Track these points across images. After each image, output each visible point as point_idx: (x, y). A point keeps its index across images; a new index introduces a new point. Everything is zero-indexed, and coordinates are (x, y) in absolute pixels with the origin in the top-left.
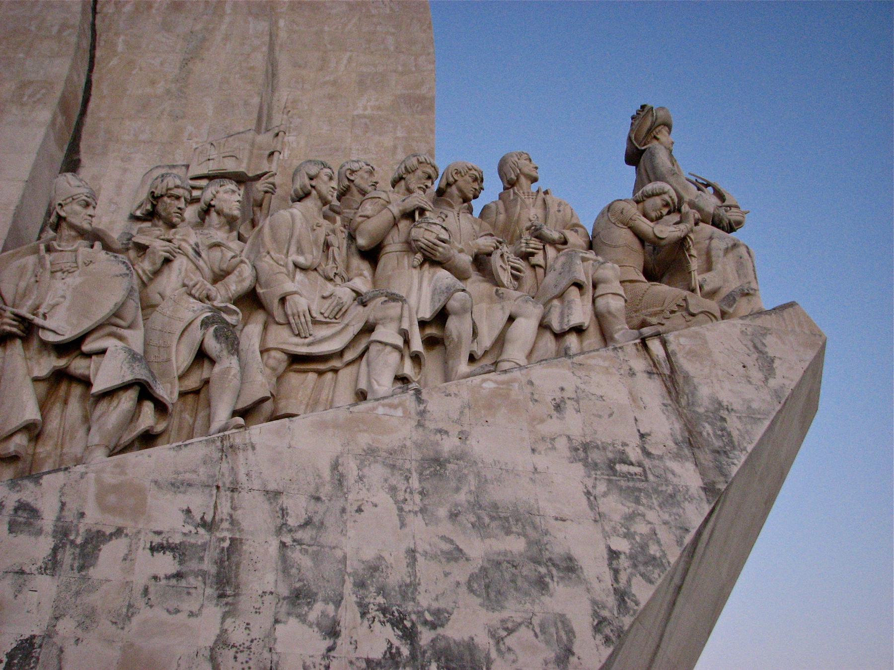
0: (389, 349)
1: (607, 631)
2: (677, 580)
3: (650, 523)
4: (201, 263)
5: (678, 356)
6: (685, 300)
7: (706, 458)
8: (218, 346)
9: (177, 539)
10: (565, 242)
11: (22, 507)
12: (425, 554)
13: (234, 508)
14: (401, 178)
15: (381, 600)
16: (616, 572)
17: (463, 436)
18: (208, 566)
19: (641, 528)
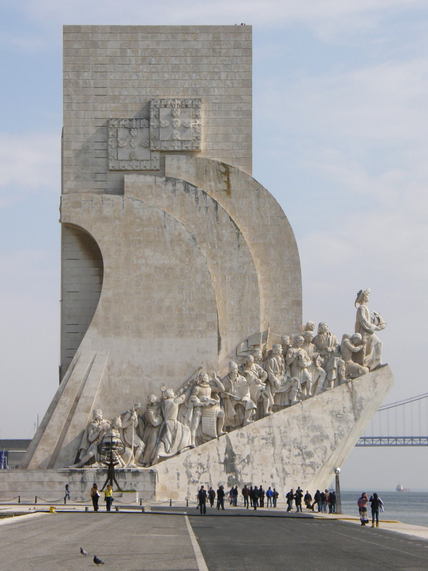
1: (333, 448)
2: (347, 436)
3: (342, 427)
4: (257, 374)
5: (355, 386)
6: (359, 369)
7: (356, 411)
9: (265, 437)
10: (333, 351)
11: (241, 434)
12: (303, 436)
13: (273, 430)
15: (297, 445)
16: (335, 438)
17: (309, 412)
18: (271, 441)
19: (341, 428)
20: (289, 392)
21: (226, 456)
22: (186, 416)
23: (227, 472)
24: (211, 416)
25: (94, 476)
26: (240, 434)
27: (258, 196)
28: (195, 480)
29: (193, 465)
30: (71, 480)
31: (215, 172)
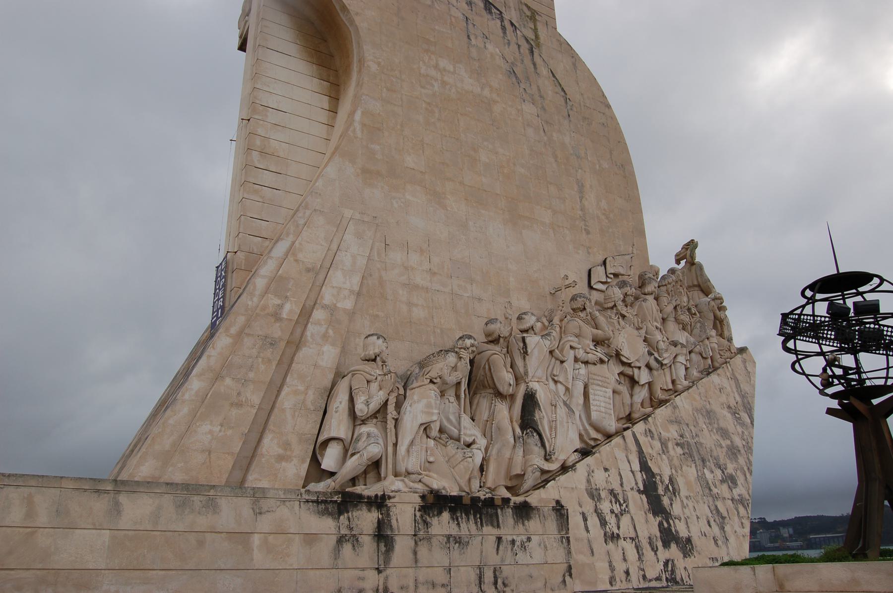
0: (683, 366)
6: (729, 347)
7: (748, 412)
8: (658, 365)
10: (695, 314)
14: (666, 285)
16: (746, 451)
18: (687, 451)
20: (670, 366)
21: (642, 475)
22: (561, 379)
23: (655, 514)
24: (605, 385)
25: (415, 516)
26: (648, 431)
27: (574, 65)
28: (613, 532)
29: (603, 494)
30: (344, 531)
31: (518, 12)
